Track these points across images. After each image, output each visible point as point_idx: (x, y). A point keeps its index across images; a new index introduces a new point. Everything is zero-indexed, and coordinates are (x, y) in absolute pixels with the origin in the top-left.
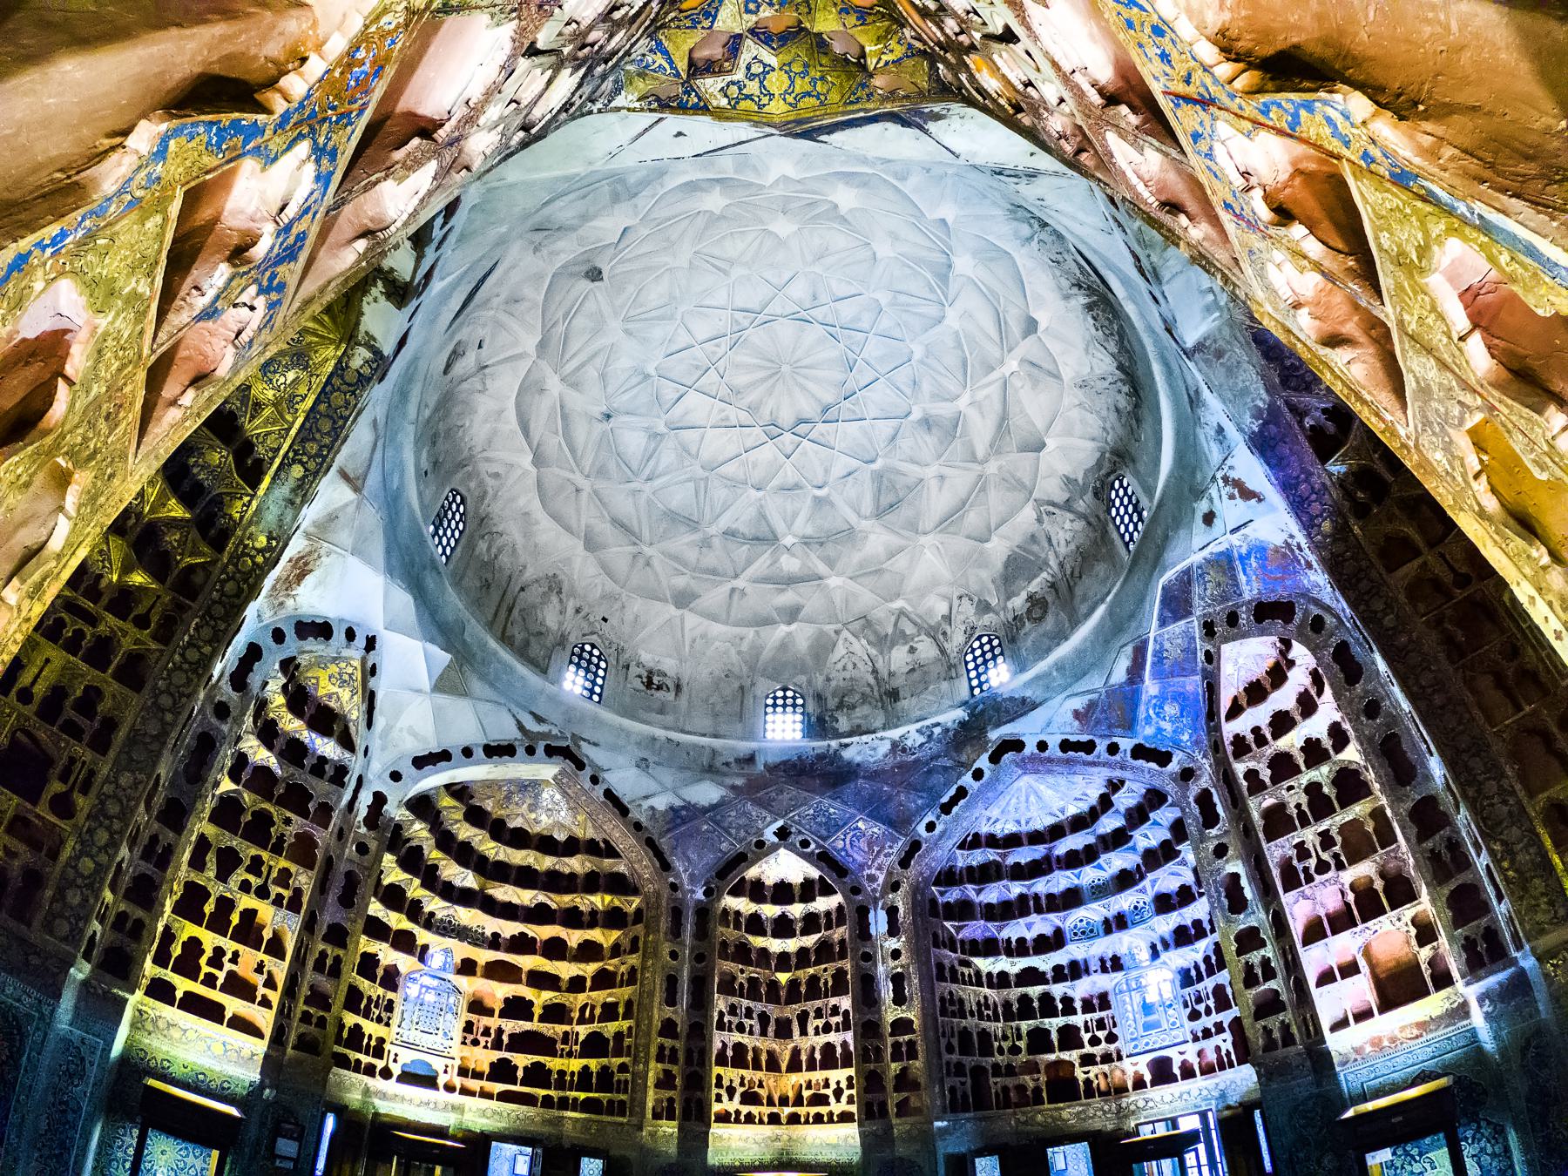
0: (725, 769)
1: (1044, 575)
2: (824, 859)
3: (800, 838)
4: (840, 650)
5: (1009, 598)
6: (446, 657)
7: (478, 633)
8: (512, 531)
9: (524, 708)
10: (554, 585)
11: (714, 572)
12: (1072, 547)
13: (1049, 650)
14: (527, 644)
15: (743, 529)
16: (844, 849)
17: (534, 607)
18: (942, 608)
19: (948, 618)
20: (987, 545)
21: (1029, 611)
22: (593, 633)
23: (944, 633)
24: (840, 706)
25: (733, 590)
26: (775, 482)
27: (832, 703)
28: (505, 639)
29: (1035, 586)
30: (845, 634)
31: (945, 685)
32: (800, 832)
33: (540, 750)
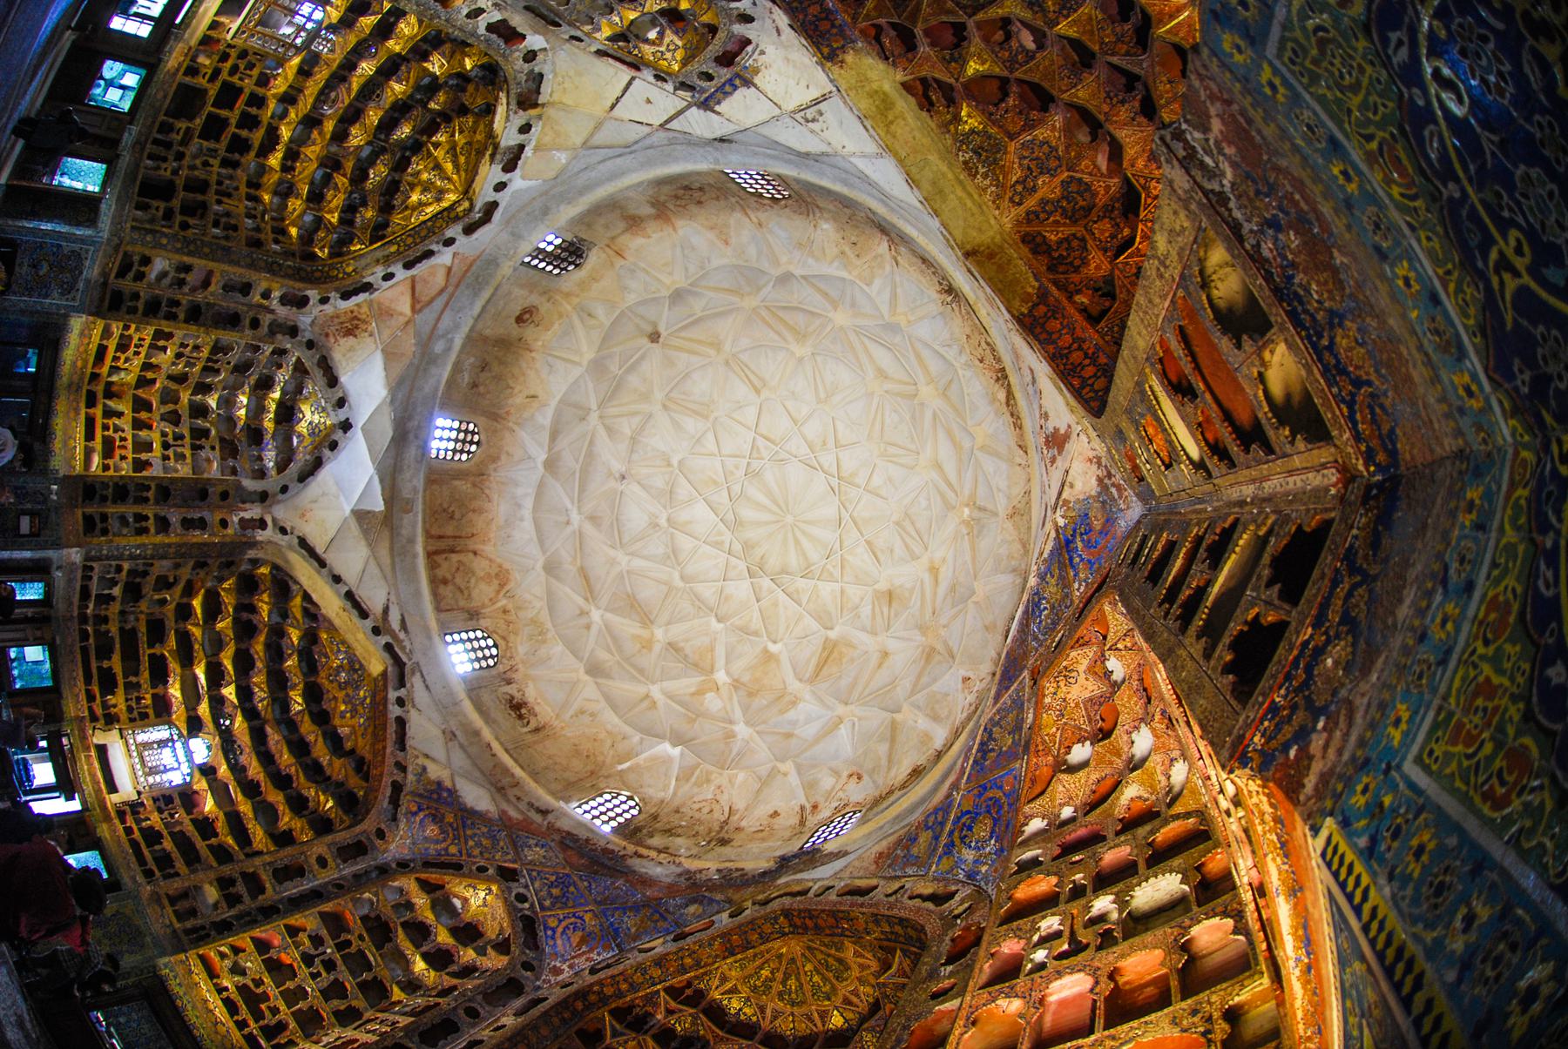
0: (514, 800)
2: (529, 926)
3: (522, 890)
6: (378, 505)
7: (415, 524)
8: (500, 508)
9: (401, 608)
10: (501, 578)
14: (445, 582)
15: (688, 651)
16: (553, 930)
17: (473, 573)
22: (504, 638)
25: (647, 696)
26: (736, 621)
28: (432, 566)
32: (526, 887)
33: (384, 639)
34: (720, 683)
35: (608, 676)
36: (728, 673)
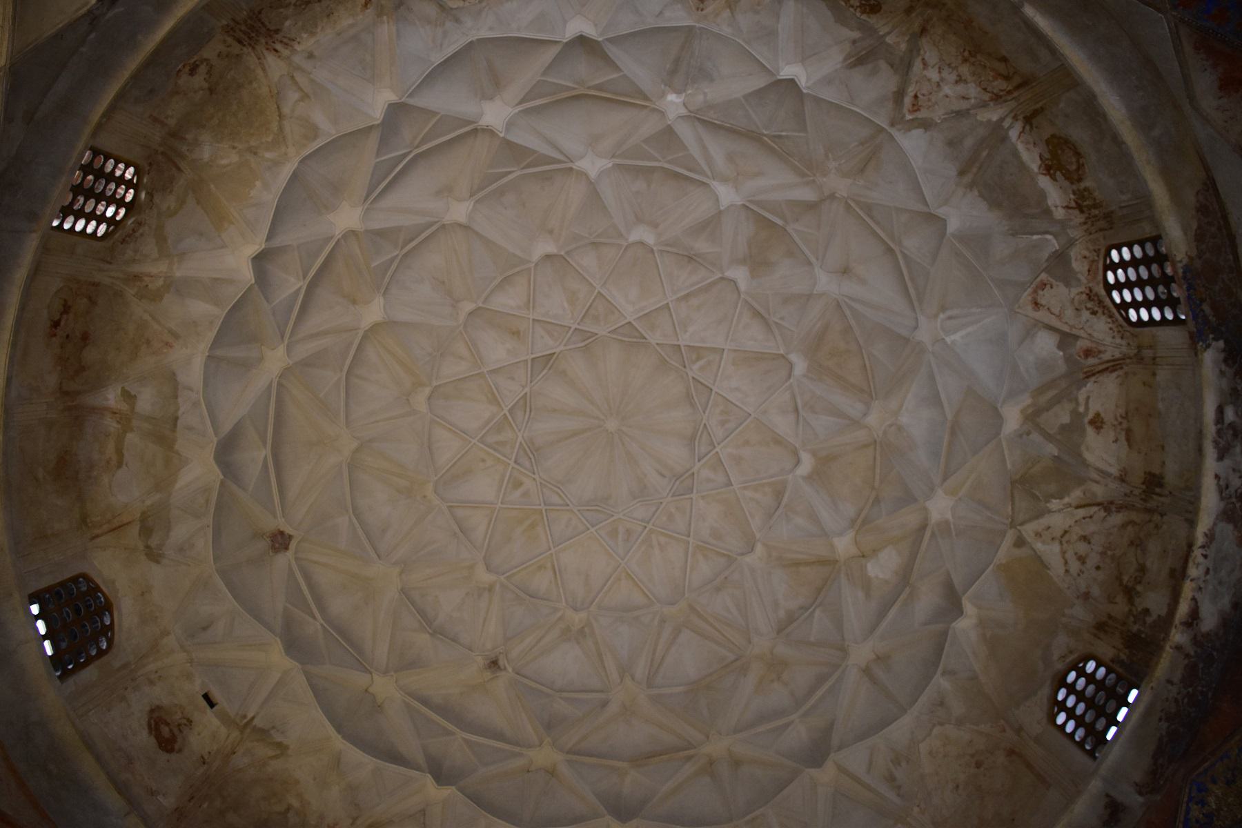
1: (1013, 134)
4: (1051, 552)
5: (1047, 212)
11: (821, 680)
12: (965, 70)
13: (1116, 140)
18: (1045, 344)
19: (1066, 339)
20: (953, 225)
21: (1068, 177)
23: (1088, 353)
24: (1130, 593)
27: (1120, 607)
29: (1031, 158)
30: (1028, 530)
31: (1163, 375)
34: (854, 551)
35: (829, 729)
36: (841, 534)
